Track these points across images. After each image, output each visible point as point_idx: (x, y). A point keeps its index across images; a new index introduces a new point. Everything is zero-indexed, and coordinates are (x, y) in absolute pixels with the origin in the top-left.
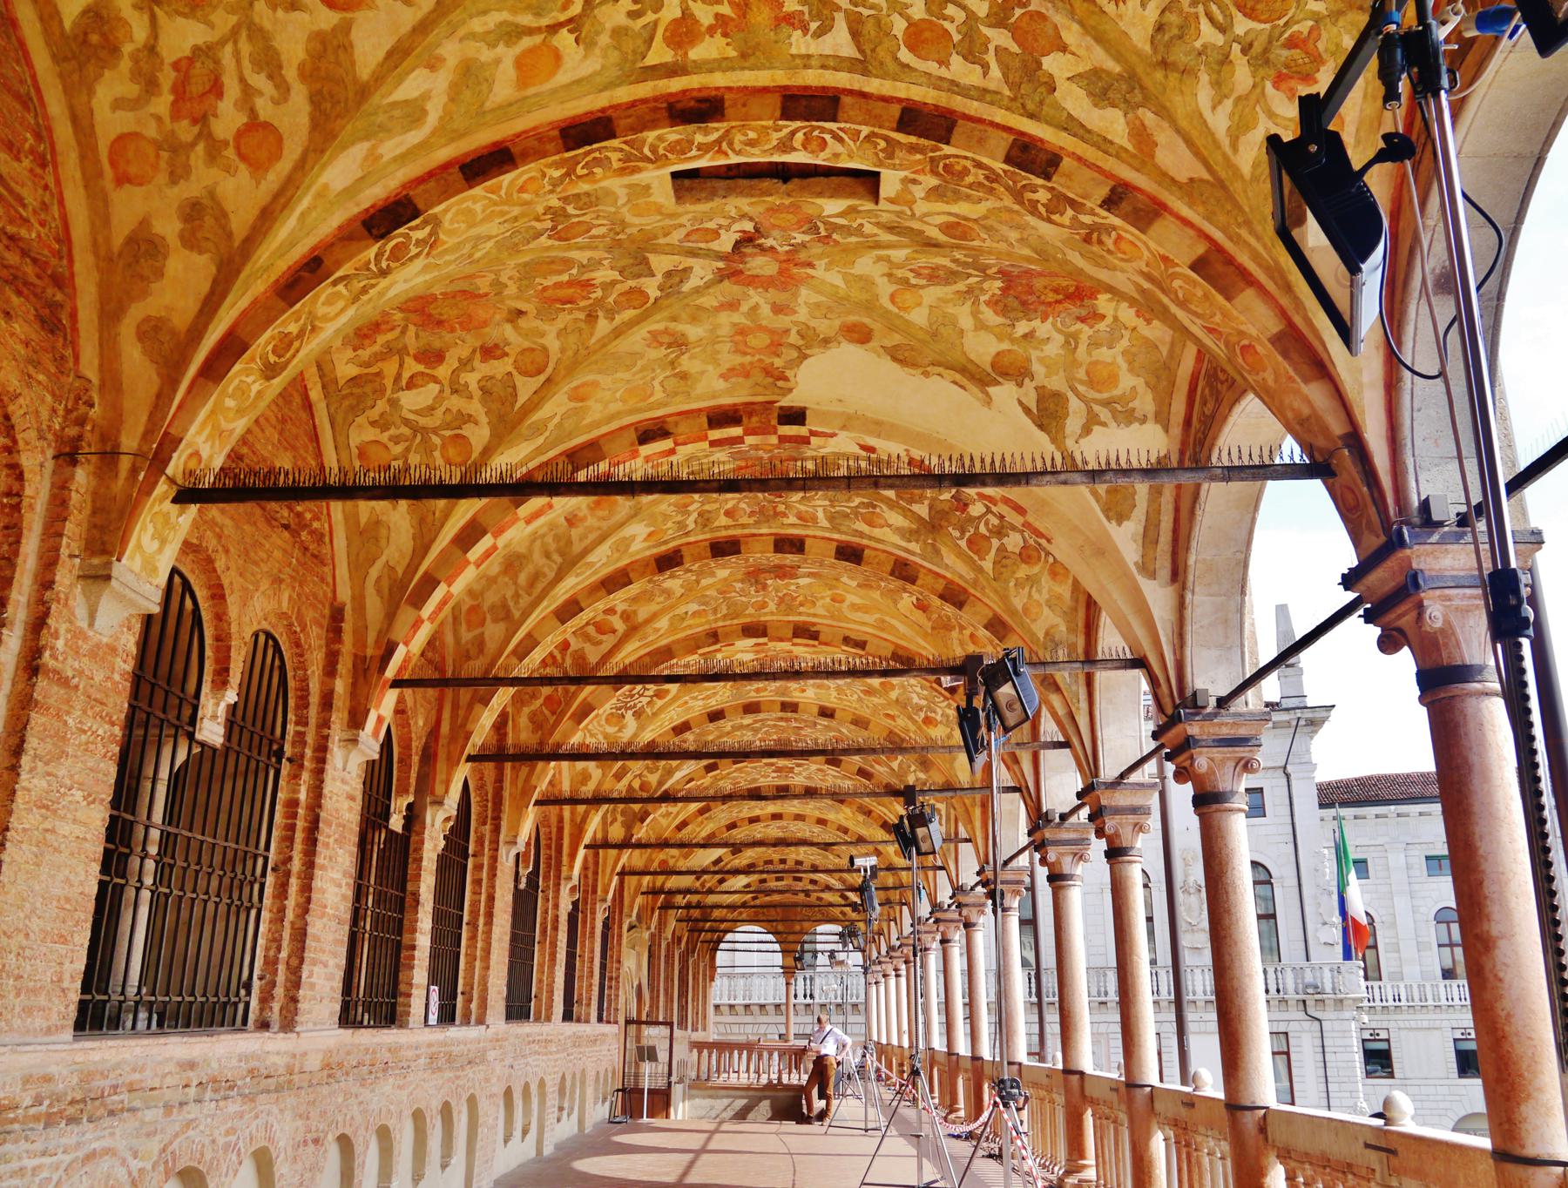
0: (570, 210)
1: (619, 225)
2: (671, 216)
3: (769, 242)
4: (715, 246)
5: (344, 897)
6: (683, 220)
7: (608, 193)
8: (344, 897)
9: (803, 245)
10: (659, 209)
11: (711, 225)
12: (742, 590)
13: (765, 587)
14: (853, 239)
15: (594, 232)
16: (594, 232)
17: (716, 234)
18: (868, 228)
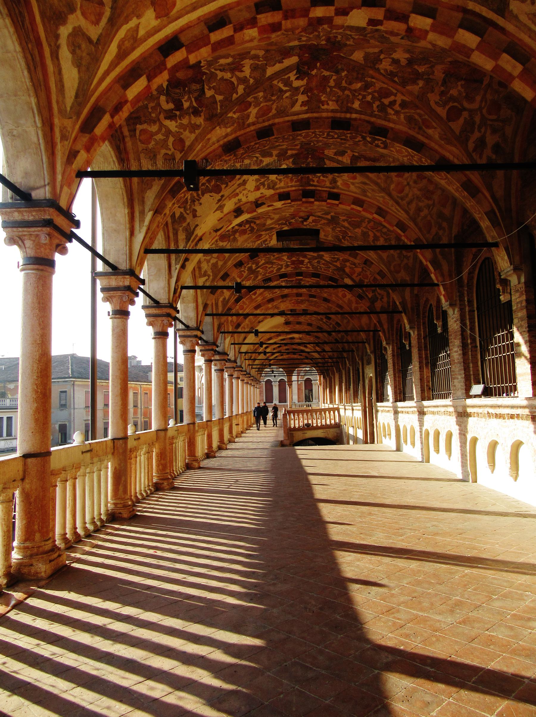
0: (341, 237)
1: (333, 229)
2: (321, 228)
3: (300, 220)
4: (314, 218)
5: (460, 355)
6: (319, 226)
7: (332, 237)
8: (460, 355)
9: (292, 219)
10: (324, 231)
11: (314, 224)
12: (348, 39)
13: (328, 39)
14: (280, 222)
15: (339, 229)
16: (339, 229)
17: (313, 221)
18: (277, 226)
